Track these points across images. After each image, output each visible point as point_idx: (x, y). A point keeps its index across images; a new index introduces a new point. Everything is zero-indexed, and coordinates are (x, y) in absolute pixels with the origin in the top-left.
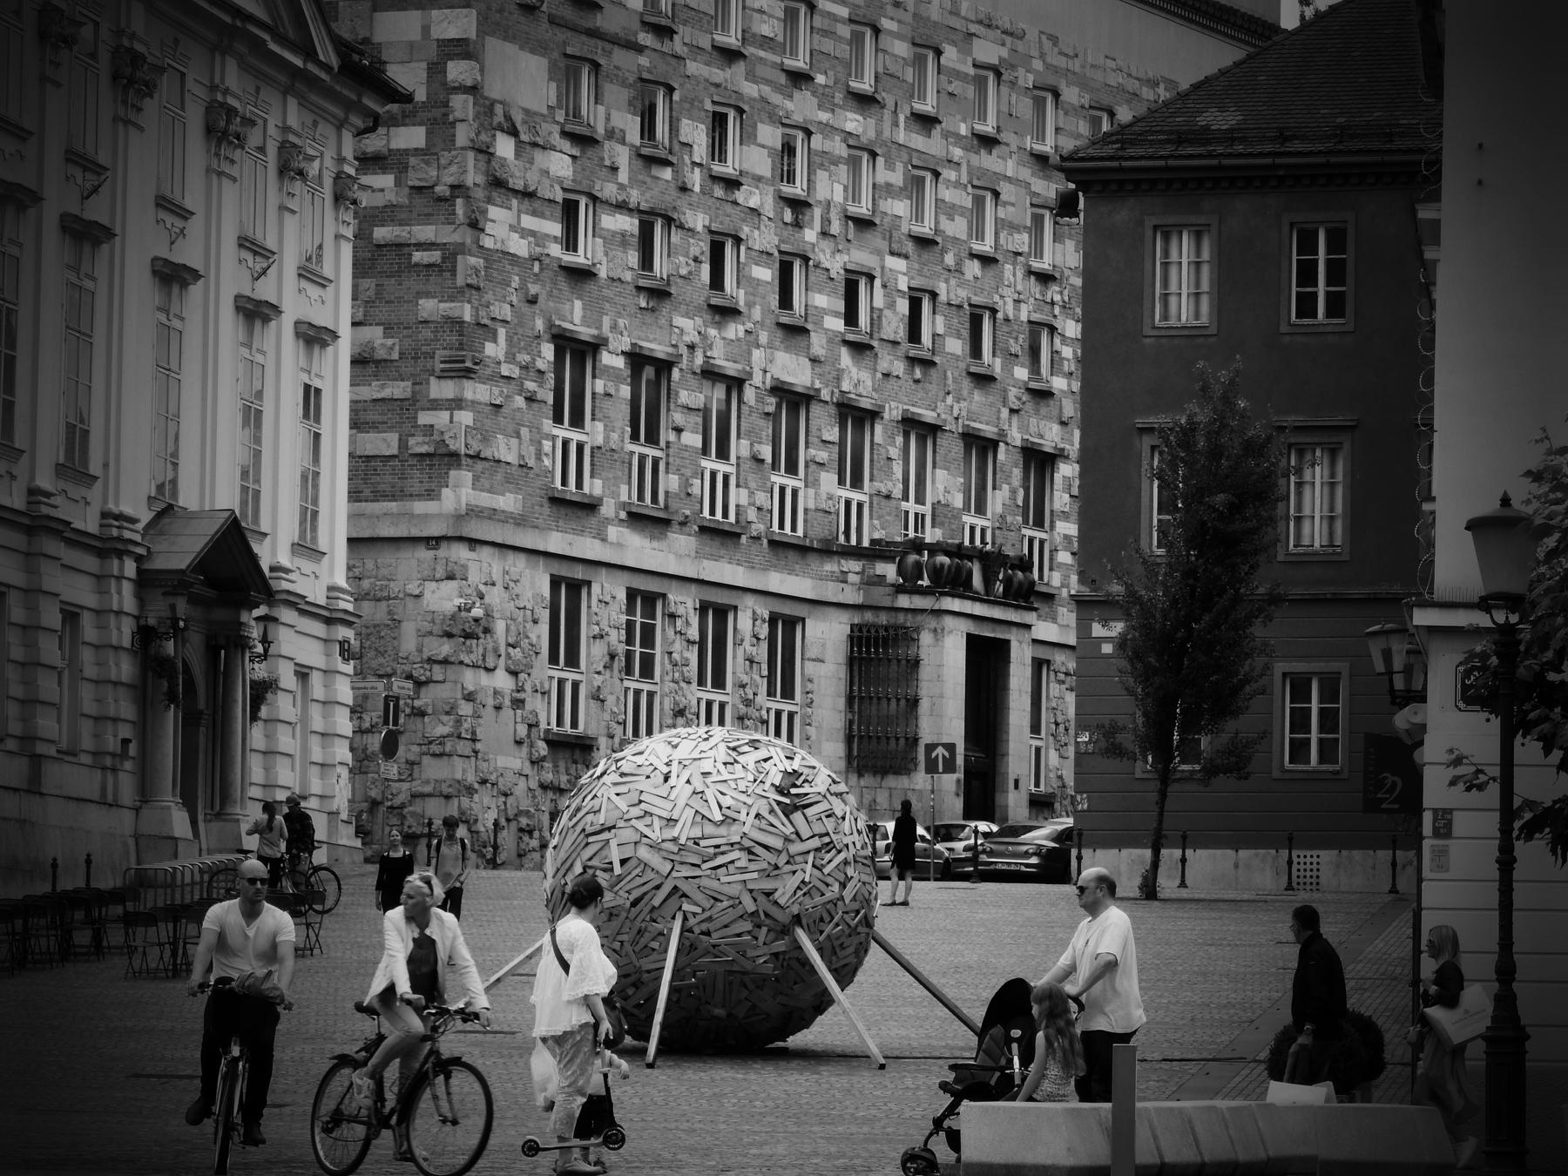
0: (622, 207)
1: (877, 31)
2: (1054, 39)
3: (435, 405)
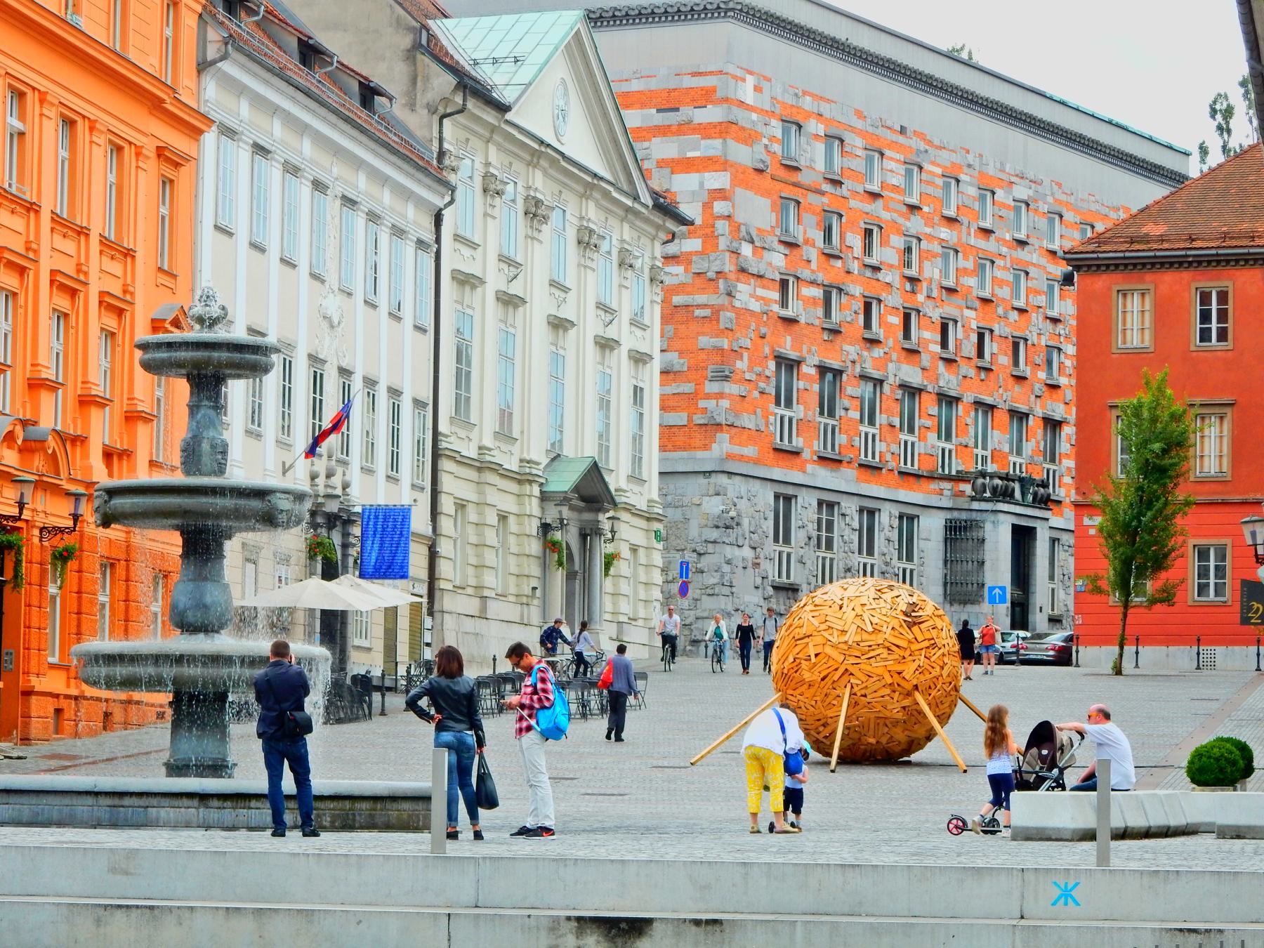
0: (813, 283)
1: (958, 181)
2: (1059, 185)
3: (708, 397)
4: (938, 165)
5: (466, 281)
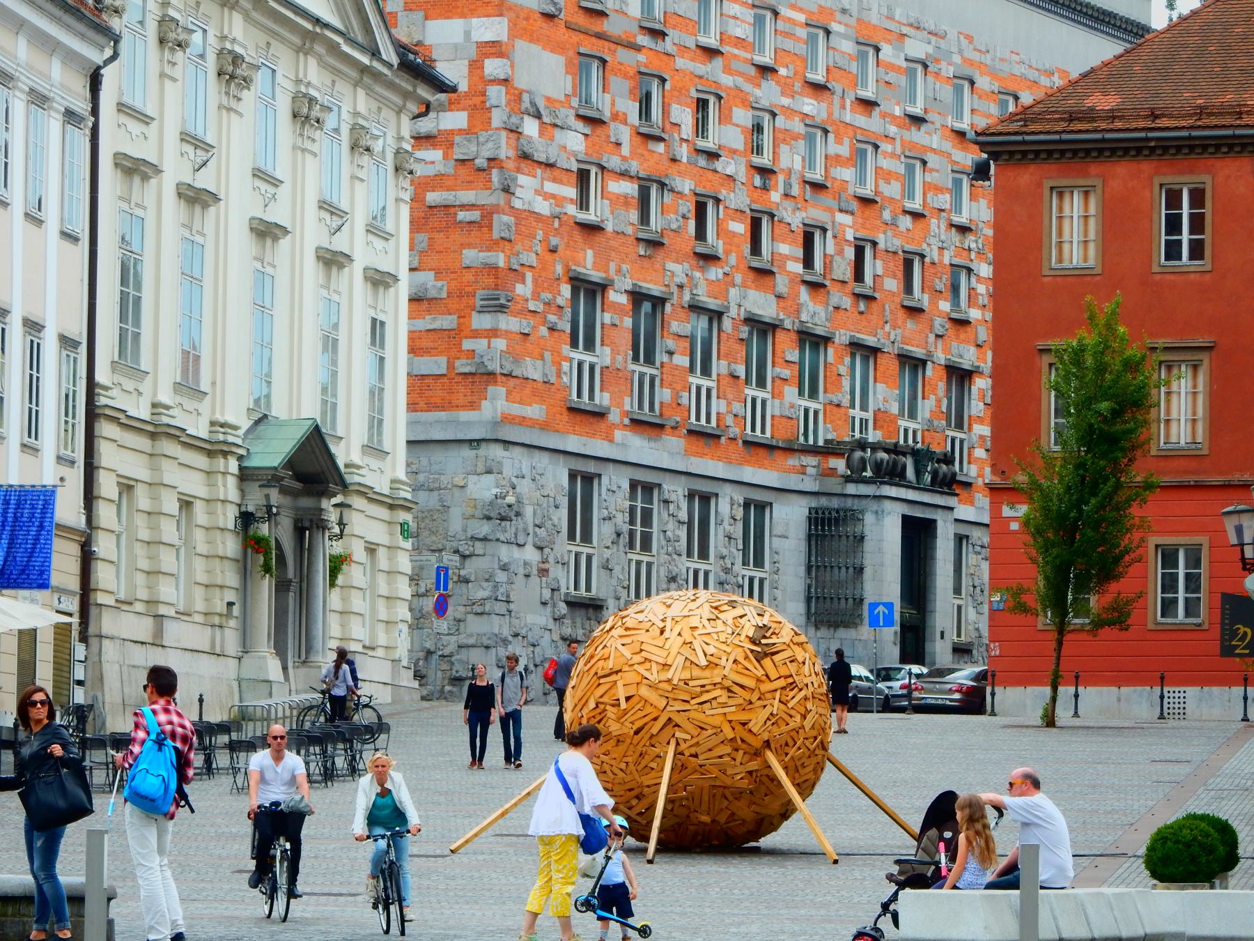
0: (624, 175)
1: (828, 32)
2: (970, 38)
3: (476, 334)
4: (801, 10)
5: (134, 169)
